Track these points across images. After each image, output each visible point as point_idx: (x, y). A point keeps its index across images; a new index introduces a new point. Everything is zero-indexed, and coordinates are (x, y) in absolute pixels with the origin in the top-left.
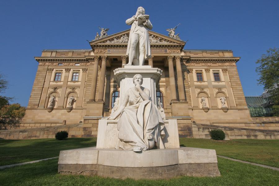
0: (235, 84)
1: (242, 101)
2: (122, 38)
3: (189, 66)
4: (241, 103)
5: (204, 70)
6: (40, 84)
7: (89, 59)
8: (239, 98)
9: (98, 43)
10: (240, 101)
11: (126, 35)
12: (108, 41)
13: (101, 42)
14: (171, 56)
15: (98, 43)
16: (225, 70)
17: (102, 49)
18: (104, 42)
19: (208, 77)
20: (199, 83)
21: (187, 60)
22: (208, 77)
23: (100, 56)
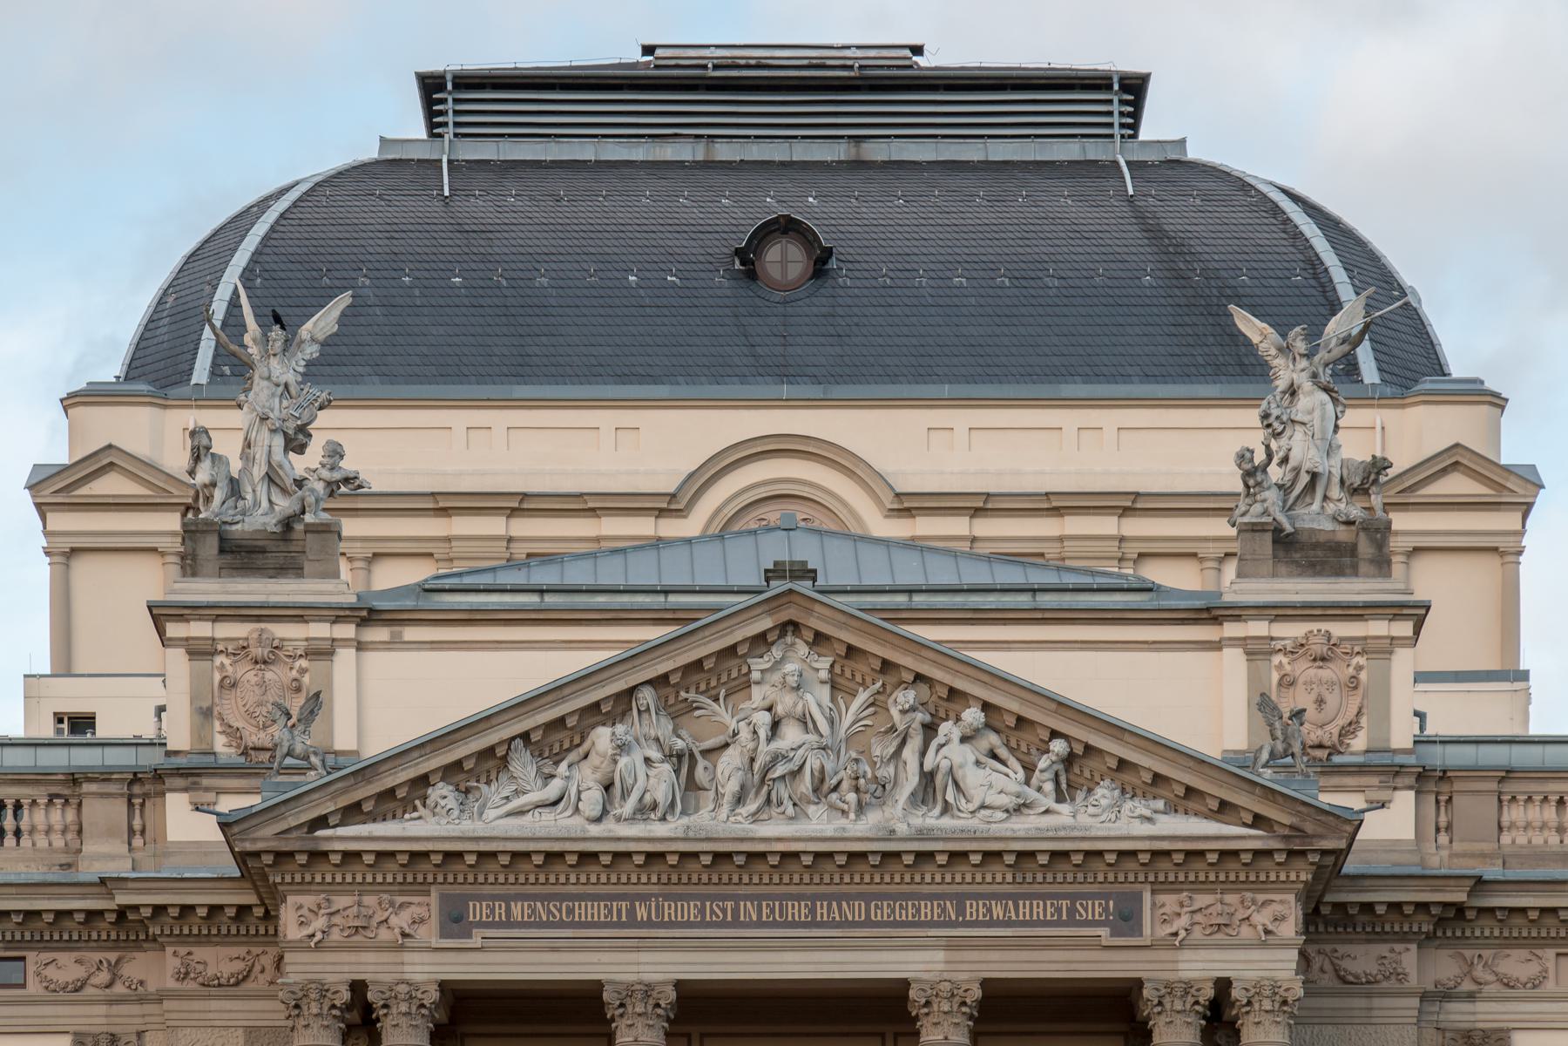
2: (602, 737)
3: (1471, 997)
7: (159, 910)
9: (321, 822)
11: (647, 696)
12: (441, 792)
13: (353, 812)
14: (1188, 987)
15: (321, 822)
17: (362, 888)
18: (390, 803)
21: (1441, 922)
23: (358, 987)
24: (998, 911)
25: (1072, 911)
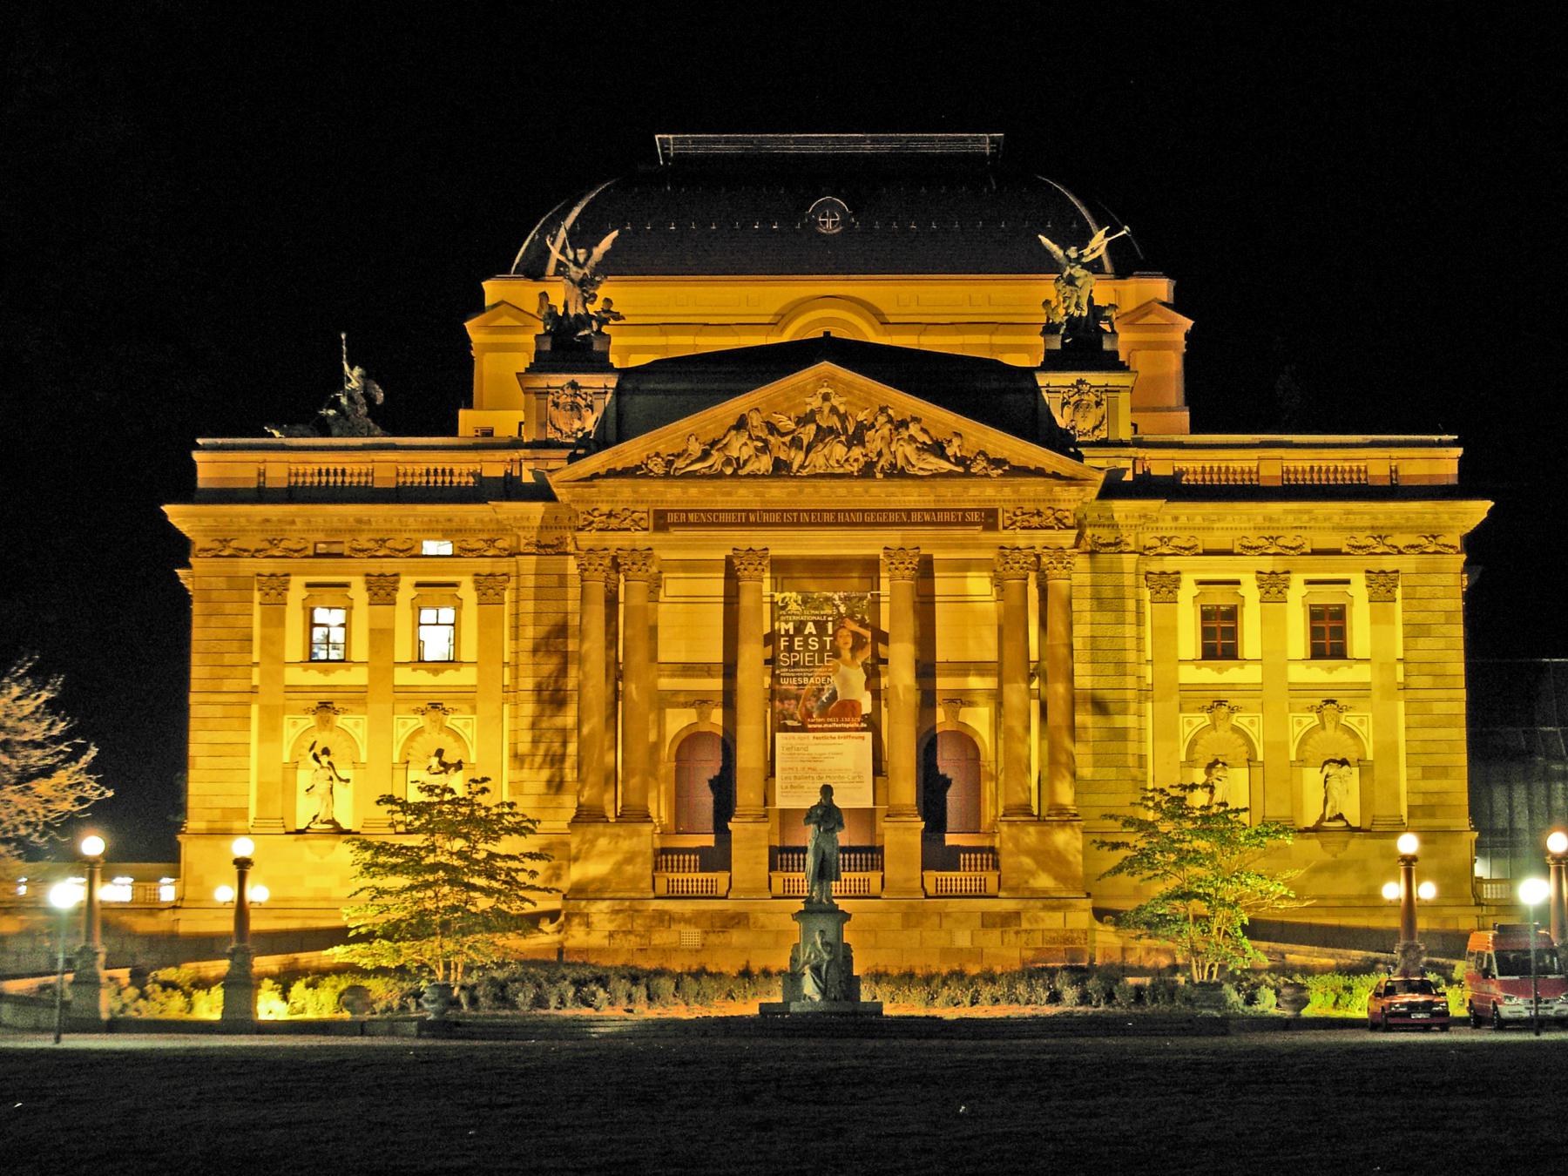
0: (1427, 681)
1: (1444, 784)
4: (1434, 800)
5: (1250, 591)
6: (228, 685)
8: (1428, 772)
10: (1433, 785)
16: (1382, 585)
19: (1273, 629)
20: (1208, 674)
22: (1275, 632)
24: (927, 518)
25: (964, 517)
